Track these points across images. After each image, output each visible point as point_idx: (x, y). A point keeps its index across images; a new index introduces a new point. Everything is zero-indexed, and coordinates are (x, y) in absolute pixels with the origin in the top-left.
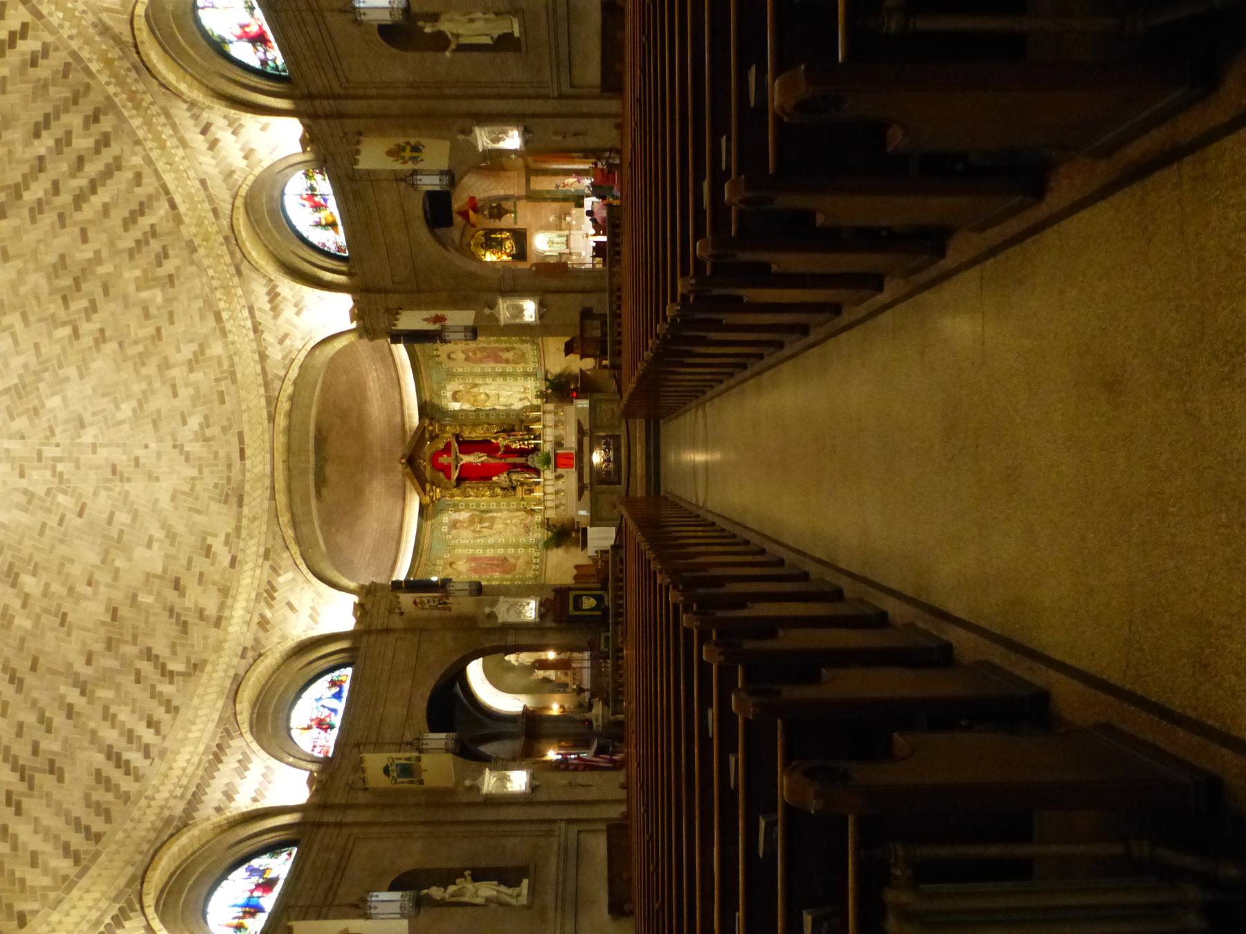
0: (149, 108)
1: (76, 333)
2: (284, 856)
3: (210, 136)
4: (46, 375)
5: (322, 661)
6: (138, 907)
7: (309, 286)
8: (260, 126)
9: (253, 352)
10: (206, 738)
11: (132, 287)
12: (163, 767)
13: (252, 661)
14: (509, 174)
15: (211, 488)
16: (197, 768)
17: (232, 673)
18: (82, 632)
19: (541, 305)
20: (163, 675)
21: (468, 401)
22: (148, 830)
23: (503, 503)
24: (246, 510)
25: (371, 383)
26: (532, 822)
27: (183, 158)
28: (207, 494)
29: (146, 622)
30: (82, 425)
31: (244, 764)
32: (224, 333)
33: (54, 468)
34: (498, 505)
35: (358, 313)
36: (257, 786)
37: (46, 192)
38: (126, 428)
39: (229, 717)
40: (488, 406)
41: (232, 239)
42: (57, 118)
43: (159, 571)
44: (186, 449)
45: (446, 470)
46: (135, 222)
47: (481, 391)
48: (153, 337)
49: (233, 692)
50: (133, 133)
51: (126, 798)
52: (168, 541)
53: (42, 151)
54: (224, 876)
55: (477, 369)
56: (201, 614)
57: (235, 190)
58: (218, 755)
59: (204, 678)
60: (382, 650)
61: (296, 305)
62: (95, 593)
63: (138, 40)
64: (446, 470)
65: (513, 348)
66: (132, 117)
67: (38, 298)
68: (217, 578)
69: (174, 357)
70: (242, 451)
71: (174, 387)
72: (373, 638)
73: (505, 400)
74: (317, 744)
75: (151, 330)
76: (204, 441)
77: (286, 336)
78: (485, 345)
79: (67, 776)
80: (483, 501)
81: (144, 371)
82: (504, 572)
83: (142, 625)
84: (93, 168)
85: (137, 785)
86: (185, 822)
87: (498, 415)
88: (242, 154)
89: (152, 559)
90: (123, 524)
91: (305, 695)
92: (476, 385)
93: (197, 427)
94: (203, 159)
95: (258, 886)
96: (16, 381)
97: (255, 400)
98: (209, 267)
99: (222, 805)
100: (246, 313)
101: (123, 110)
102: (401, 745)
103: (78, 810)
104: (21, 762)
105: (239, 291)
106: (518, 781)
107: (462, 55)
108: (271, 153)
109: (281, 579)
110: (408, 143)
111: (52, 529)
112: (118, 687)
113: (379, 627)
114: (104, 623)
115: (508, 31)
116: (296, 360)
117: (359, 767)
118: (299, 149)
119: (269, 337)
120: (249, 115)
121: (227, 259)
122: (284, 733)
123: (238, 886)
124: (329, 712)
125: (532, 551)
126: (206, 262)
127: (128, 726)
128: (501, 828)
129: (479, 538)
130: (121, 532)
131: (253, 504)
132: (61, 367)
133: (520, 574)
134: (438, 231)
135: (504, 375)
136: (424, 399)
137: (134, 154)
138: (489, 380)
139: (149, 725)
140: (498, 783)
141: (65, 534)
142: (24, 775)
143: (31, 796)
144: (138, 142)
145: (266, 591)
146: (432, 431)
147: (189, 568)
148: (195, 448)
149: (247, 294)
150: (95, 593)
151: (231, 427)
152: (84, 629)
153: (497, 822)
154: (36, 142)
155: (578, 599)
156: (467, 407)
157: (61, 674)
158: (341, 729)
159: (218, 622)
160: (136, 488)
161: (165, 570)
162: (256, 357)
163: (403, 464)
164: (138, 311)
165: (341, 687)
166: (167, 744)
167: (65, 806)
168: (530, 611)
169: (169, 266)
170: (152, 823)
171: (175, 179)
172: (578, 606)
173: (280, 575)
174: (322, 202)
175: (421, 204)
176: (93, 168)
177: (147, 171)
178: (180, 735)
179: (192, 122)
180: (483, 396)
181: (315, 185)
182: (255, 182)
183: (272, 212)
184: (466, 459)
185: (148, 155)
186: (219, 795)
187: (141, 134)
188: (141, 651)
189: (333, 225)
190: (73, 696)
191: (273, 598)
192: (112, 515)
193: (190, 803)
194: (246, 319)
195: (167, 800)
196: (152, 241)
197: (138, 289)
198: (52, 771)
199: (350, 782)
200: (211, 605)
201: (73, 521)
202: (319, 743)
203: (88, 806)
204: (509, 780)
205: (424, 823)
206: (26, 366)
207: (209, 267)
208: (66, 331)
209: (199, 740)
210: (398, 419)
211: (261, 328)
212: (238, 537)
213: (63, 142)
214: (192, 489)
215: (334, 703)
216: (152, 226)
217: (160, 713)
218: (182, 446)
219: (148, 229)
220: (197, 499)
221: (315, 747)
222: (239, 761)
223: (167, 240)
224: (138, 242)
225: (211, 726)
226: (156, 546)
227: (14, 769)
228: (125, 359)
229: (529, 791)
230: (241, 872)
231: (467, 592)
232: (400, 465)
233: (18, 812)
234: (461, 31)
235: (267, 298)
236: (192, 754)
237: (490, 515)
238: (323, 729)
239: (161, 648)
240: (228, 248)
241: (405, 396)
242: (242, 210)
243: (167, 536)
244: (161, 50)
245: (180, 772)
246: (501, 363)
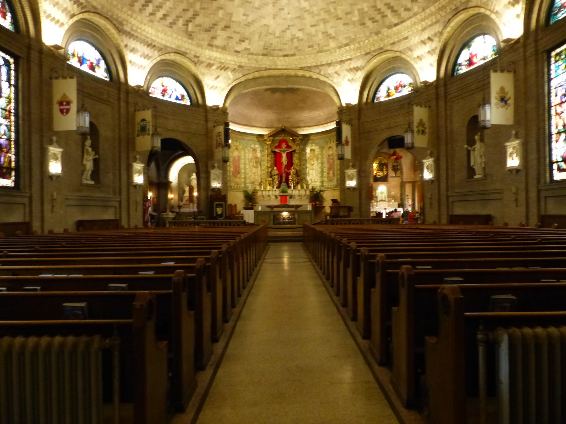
0: (439, 14)
2: (106, 75)
3: (427, 41)
5: (193, 91)
6: (83, 11)
8: (432, 63)
10: (158, 40)
11: (359, 7)
12: (145, 21)
13: (193, 60)
15: (271, 42)
17: (188, 51)
19: (354, 189)
21: (310, 156)
22: (117, 15)
23: (264, 172)
24: (261, 57)
25: (318, 113)
26: (120, 185)
29: (210, 14)
31: (147, 57)
32: (340, 47)
34: (264, 170)
35: (349, 107)
36: (136, 63)
38: (297, 4)
39: (168, 50)
40: (308, 165)
41: (382, 51)
43: (233, 19)
45: (279, 146)
48: (337, 16)
49: (179, 52)
50: (428, 8)
52: (246, 23)
54: (96, 48)
55: (325, 160)
56: (214, 38)
57: (403, 52)
58: (151, 45)
59: (185, 39)
61: (352, 79)
63: (469, 9)
64: (279, 146)
65: (334, 176)
68: (230, 44)
69: (329, 25)
70: (287, 56)
73: (311, 172)
75: (340, 16)
78: (336, 164)
81: (322, 12)
86: (120, 31)
87: (304, 169)
88: (420, 55)
89: (238, 16)
91: (178, 84)
92: (317, 159)
93: (297, 35)
94: (417, 38)
95: (92, 63)
97: (310, 61)
98: (369, 41)
100: (349, 57)
102: (155, 127)
105: (358, 54)
106: (139, 179)
107: (465, 153)
108: (420, 68)
110: (426, 128)
113: (209, 117)
115: (477, 173)
117: (145, 108)
118: (422, 80)
119: (338, 67)
120: (437, 58)
121: (373, 49)
122: (161, 74)
123: (92, 55)
125: (243, 185)
126: (371, 39)
127: (164, 6)
128: (117, 172)
129: (249, 161)
131: (263, 61)
134: (386, 143)
135: (322, 172)
136: (311, 136)
137: (419, 8)
138: (320, 165)
140: (138, 170)
144: (424, 10)
145: (224, 67)
146: (296, 140)
147: (235, 32)
148: (288, 35)
149: (357, 57)
153: (120, 170)
155: (221, 206)
156: (308, 155)
158: (162, 100)
159: (210, 45)
160: (270, 9)
161: (233, 22)
162: (329, 62)
164: (349, 10)
165: (181, 100)
166: (156, 23)
168: (216, 184)
169: (369, 23)
170: (121, 17)
171: (408, 26)
172: (218, 206)
173: (232, 72)
175: (399, 134)
177: (411, 13)
178: (160, 29)
179: (433, 33)
180: (313, 163)
181: (406, 87)
182: (407, 61)
183: (394, 68)
184: (284, 156)
187: (428, 11)
188: (197, 11)
189: (389, 95)
191: (221, 69)
193: (129, 33)
195: (131, 23)
196: (380, 16)
197: (359, 10)
199: (138, 104)
200: (218, 42)
202: (156, 91)
204: (139, 175)
205: (120, 137)
207: (369, 41)
209: (158, 37)
210: (302, 125)
211: (342, 64)
216: (387, 16)
217: (169, 20)
219: (385, 14)
220: (265, 36)
221: (154, 88)
223: (381, 22)
224: (379, 10)
225: (164, 42)
226: (244, 18)
229: (134, 184)
230: (98, 55)
232: (281, 126)
234: (476, 152)
235: (355, 66)
236: (151, 34)
238: (162, 92)
239: (198, 20)
240: (378, 49)
241: (313, 127)
242: (395, 55)
243: (249, 23)
244: (465, 19)
246: (328, 170)
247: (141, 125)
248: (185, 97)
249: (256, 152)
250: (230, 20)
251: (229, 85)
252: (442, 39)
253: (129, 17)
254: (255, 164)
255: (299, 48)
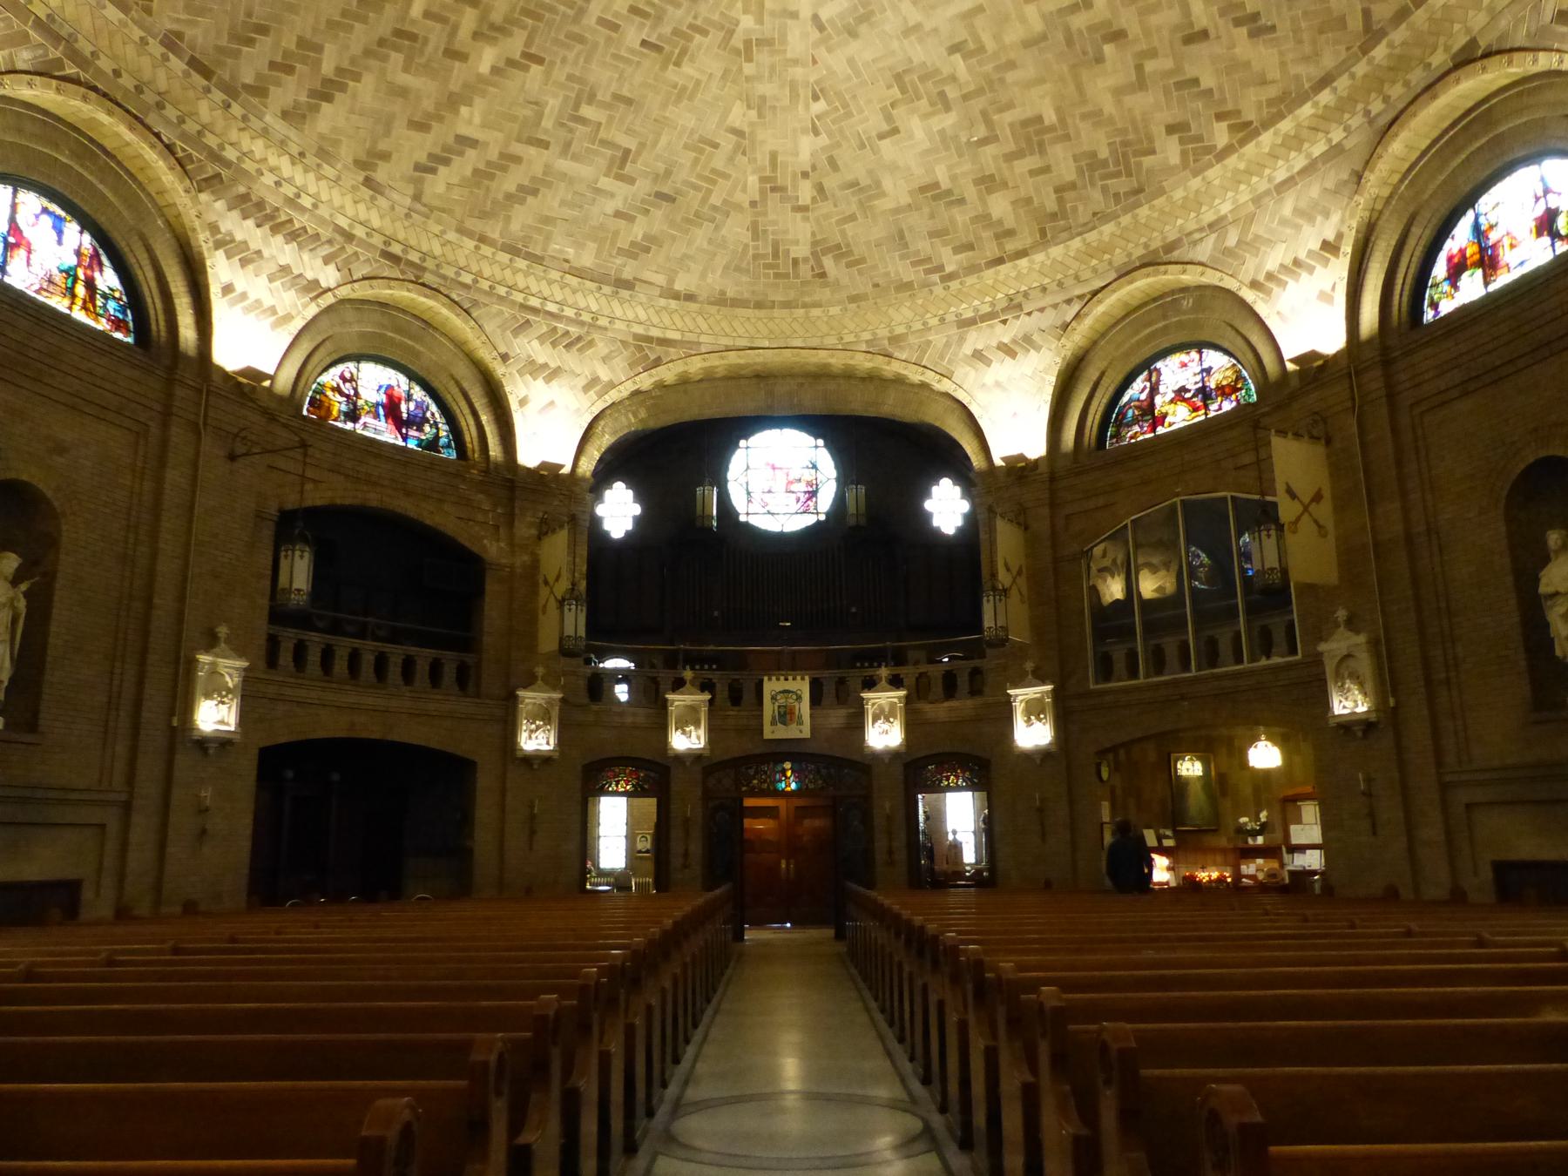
7: (1053, 395)
19: (1042, 757)
229: (196, 736)
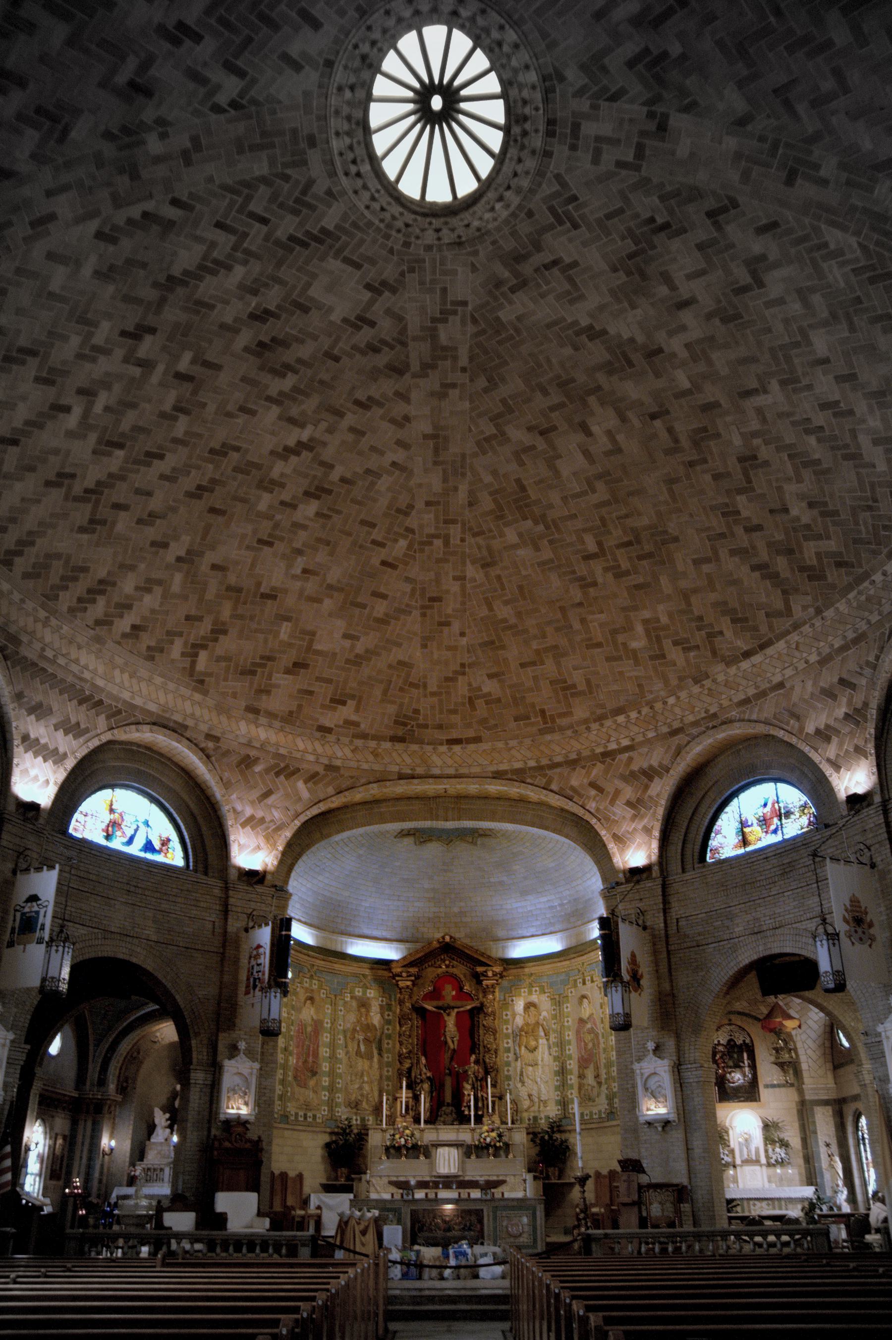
1: (588, 557)
4: (541, 527)
8: (861, 743)
9: (579, 753)
10: (115, 691)
11: (646, 614)
13: (203, 745)
14: (830, 1075)
15: (414, 706)
16: (75, 675)
17: (190, 723)
18: (250, 561)
20: (194, 646)
24: (387, 745)
25: (544, 899)
27: (807, 662)
28: (406, 700)
29: (256, 631)
30: (485, 566)
31: (72, 729)
33: (437, 536)
34: (388, 1064)
36: (43, 741)
37: (748, 519)
41: (714, 721)
42: (835, 524)
43: (317, 646)
44: (460, 678)
45: (435, 994)
46: (724, 613)
47: (541, 1041)
51: (50, 597)
52: (352, 657)
53: (794, 512)
55: (570, 1035)
56: (265, 691)
59: (184, 691)
60: (202, 904)
61: (639, 801)
62: (294, 577)
65: (600, 1084)
66: (849, 602)
67: (627, 516)
71: (533, 664)
72: (217, 892)
74: (88, 818)
76: (470, 698)
77: (600, 790)
79: (85, 537)
80: (394, 1044)
82: (296, 1069)
83: (254, 626)
84: (781, 564)
85: (65, 609)
87: (508, 1064)
90: (373, 608)
91: (155, 809)
93: (485, 690)
96: (533, 498)
99: (25, 699)
100: (625, 742)
101: (855, 592)
102: (62, 919)
103: (42, 544)
104: (106, 491)
105: (651, 735)
109: (300, 785)
111: (369, 533)
112: (185, 598)
113: (232, 901)
114: (259, 584)
116: (571, 803)
119: (597, 770)
121: (691, 718)
124: (129, 835)
125: (324, 1111)
126: (683, 695)
129: (345, 1037)
130: (364, 606)
131: (394, 754)
132: (551, 542)
133: (293, 1093)
134: (752, 977)
135: (562, 1072)
137: (805, 608)
139: (134, 627)
141: (361, 547)
142: (93, 493)
143: (66, 498)
144: (819, 612)
145: (287, 766)
147: (319, 679)
148: (462, 688)
150: (294, 577)
151: (489, 729)
152: (253, 565)
154: (804, 504)
157: (203, 538)
158: (107, 848)
159: (253, 710)
160: (413, 622)
161: (319, 653)
162: (573, 756)
163: (443, 938)
165: (159, 852)
166: (110, 644)
167: (50, 531)
169: (675, 654)
171: (780, 654)
173: (306, 782)
174: (773, 827)
175: (788, 950)
176: (781, 564)
177: (788, 623)
181: (792, 816)
184: (451, 1022)
185: (805, 623)
186: (38, 698)
187: (829, 613)
188: (224, 624)
189: (745, 842)
190: (177, 549)
191: (277, 774)
192: (384, 597)
193: (35, 664)
194: (618, 743)
197: (645, 622)
198: (92, 521)
199: (28, 852)
201: (377, 557)
203: (48, 556)
206: (551, 506)
207: (678, 698)
208: (591, 546)
211: (608, 760)
212: (356, 736)
213: (810, 533)
214: (412, 685)
215: (140, 842)
216: (721, 633)
218: (464, 674)
220: (401, 689)
222: (78, 724)
224: (700, 618)
225: (126, 695)
226: (347, 643)
227: (99, 483)
228: (562, 609)
231: (265, 1016)
232: (438, 935)
233: (48, 484)
235: (645, 765)
236: (94, 672)
237: (375, 1052)
238: (108, 826)
239: (227, 644)
240: (703, 719)
243: (357, 656)
245: (73, 657)
246: (579, 1067)
247: (23, 914)
248: (171, 845)
249: (368, 1011)
250: (309, 648)
251: (297, 816)
252: (879, 682)
253: (39, 625)
254: (363, 1048)
255: (492, 722)
